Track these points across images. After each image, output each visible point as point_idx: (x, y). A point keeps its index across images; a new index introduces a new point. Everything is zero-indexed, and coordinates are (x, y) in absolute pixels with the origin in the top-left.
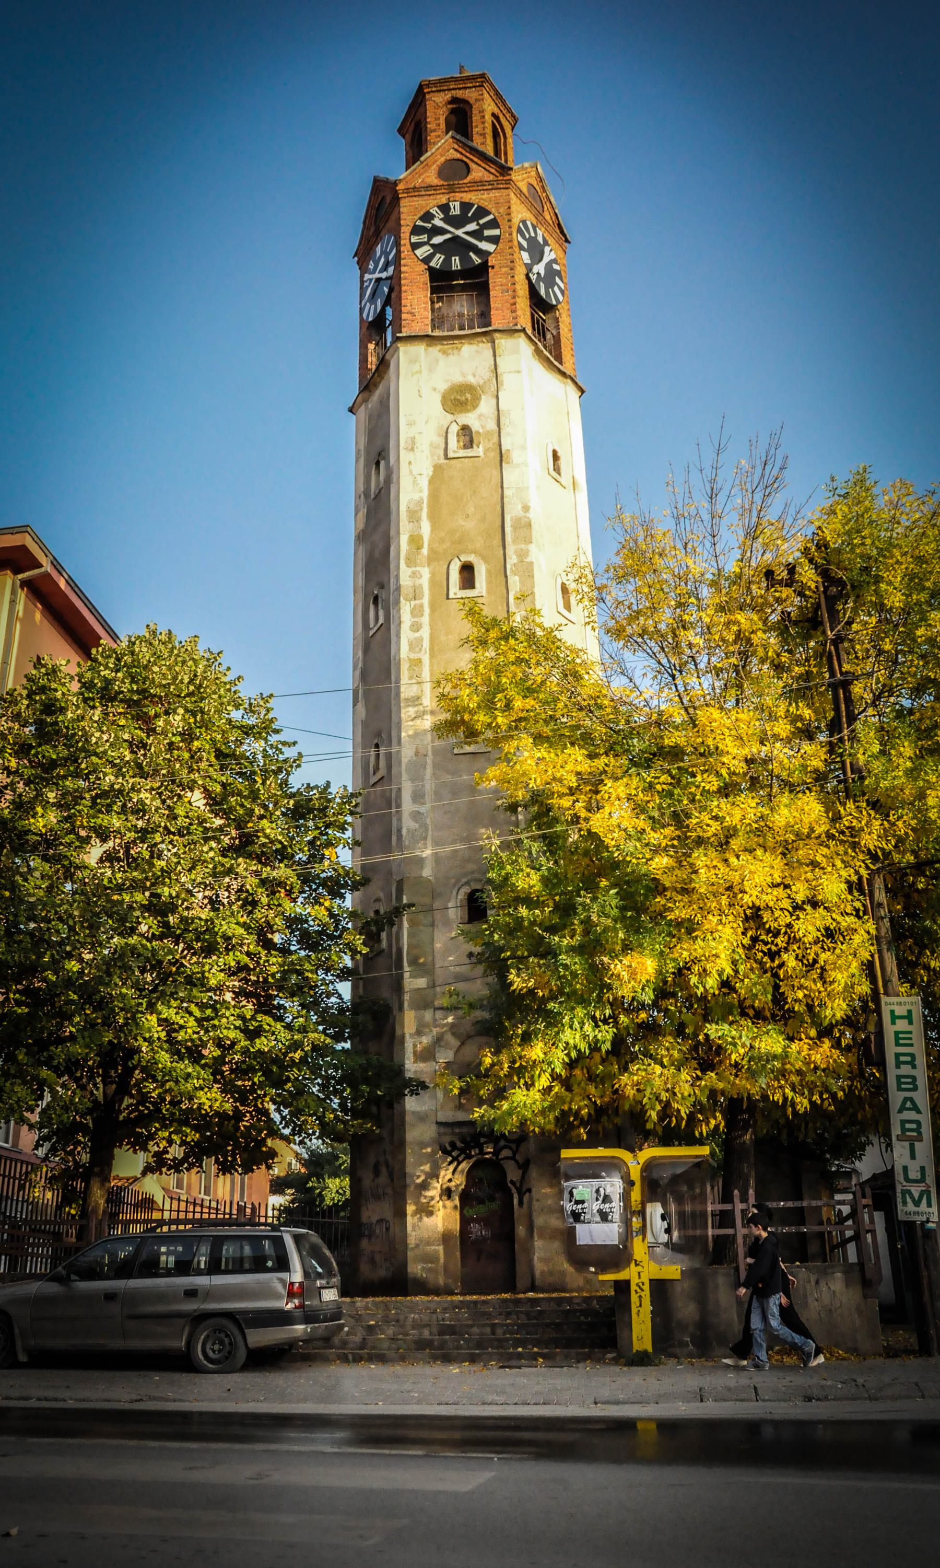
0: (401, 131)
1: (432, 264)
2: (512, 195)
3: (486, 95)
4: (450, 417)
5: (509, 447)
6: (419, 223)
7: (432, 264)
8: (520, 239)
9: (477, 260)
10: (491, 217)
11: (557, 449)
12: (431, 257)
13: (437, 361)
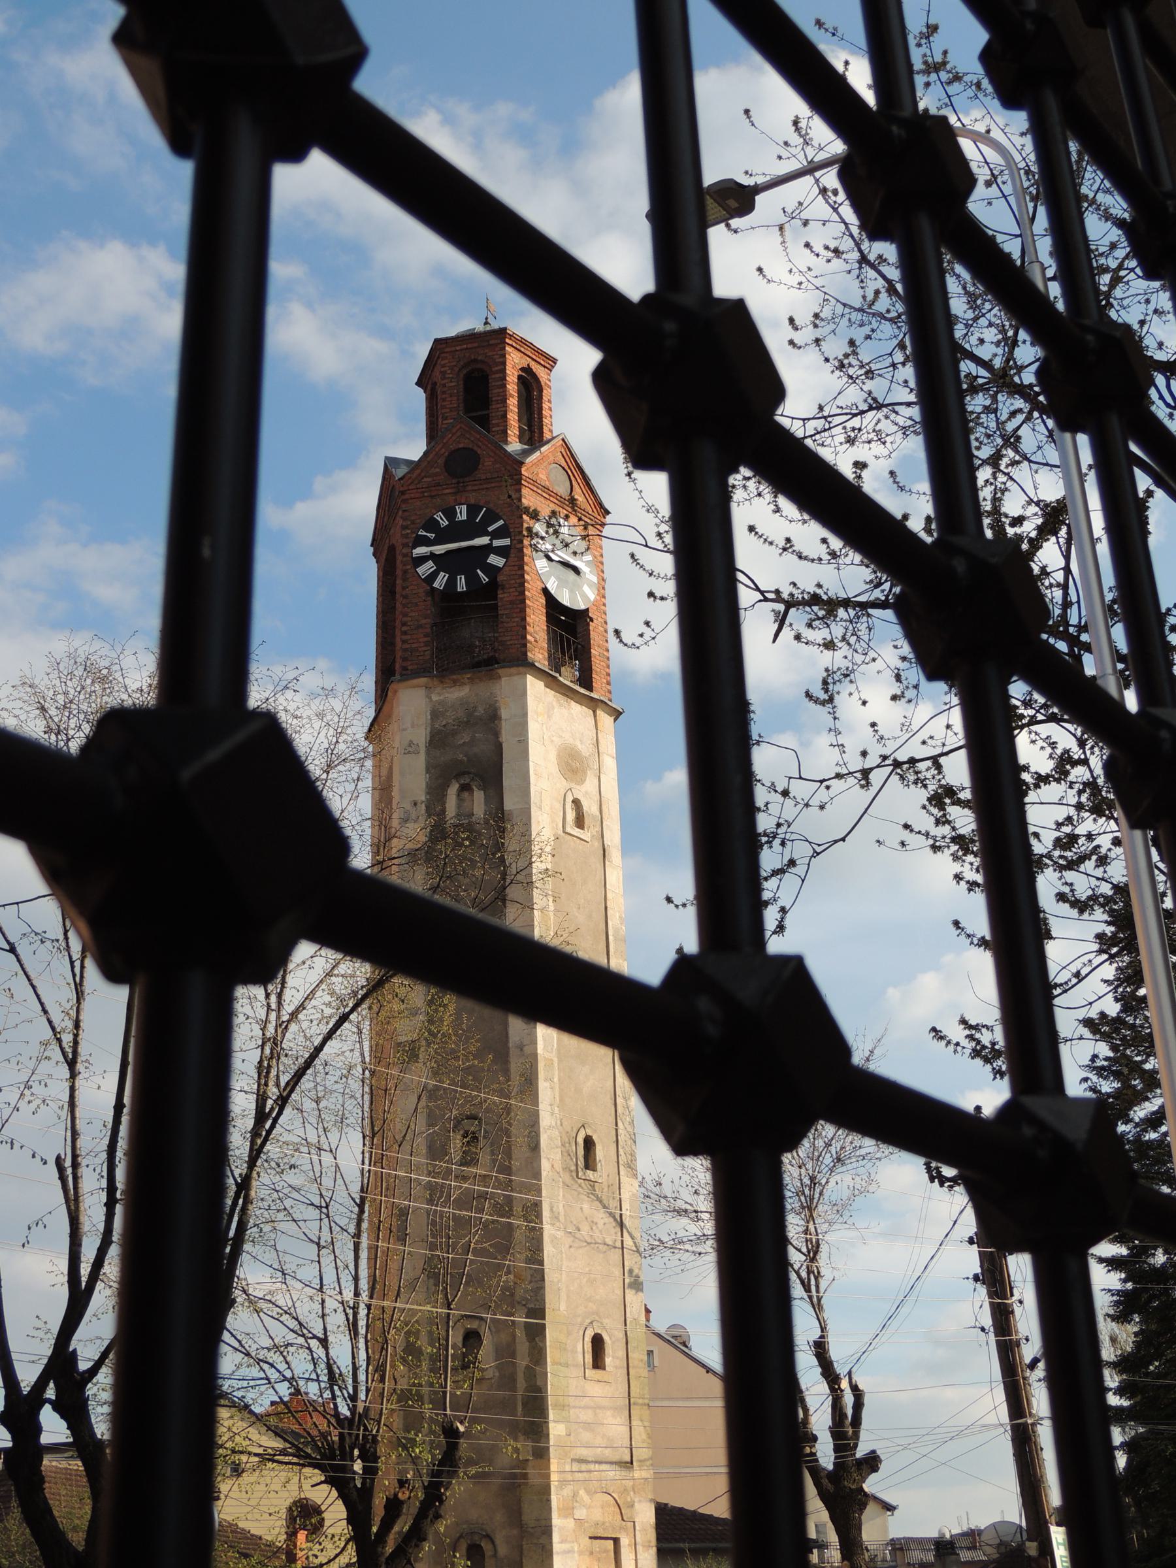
0: (419, 384)
1: (436, 585)
6: (422, 533)
7: (436, 585)
9: (485, 579)
10: (501, 522)
12: (433, 577)
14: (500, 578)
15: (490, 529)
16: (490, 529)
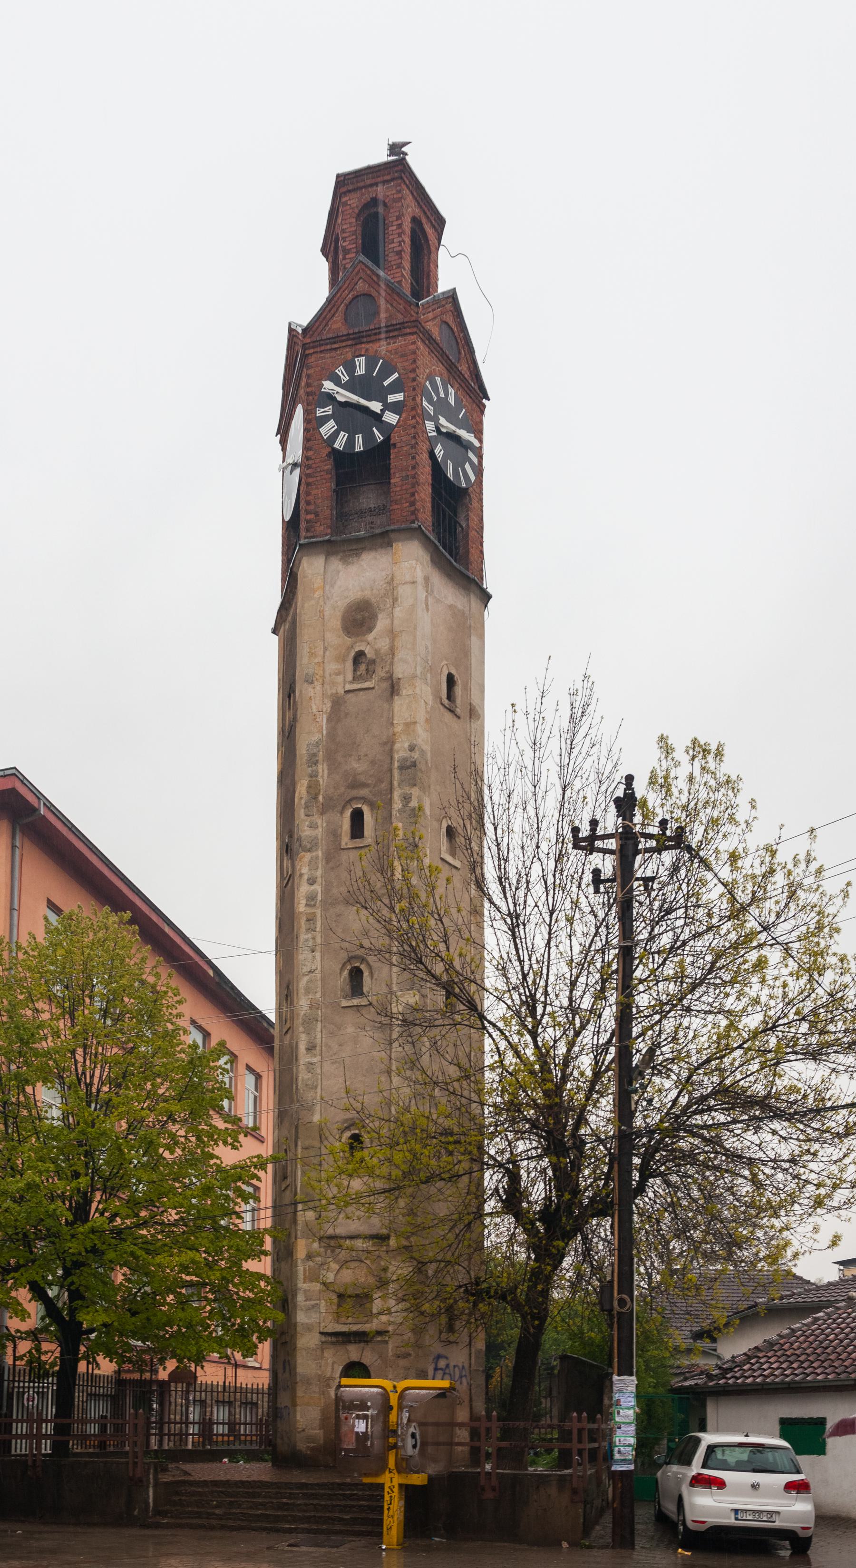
1: (336, 446)
2: (419, 343)
3: (406, 192)
4: (349, 641)
5: (400, 676)
8: (425, 403)
9: (379, 437)
10: (396, 375)
11: (453, 672)
13: (338, 572)
14: (395, 438)
15: (386, 383)
16: (386, 383)
